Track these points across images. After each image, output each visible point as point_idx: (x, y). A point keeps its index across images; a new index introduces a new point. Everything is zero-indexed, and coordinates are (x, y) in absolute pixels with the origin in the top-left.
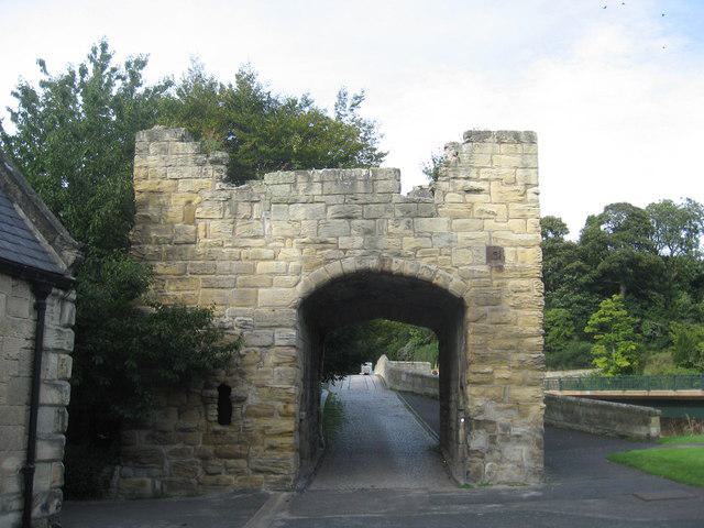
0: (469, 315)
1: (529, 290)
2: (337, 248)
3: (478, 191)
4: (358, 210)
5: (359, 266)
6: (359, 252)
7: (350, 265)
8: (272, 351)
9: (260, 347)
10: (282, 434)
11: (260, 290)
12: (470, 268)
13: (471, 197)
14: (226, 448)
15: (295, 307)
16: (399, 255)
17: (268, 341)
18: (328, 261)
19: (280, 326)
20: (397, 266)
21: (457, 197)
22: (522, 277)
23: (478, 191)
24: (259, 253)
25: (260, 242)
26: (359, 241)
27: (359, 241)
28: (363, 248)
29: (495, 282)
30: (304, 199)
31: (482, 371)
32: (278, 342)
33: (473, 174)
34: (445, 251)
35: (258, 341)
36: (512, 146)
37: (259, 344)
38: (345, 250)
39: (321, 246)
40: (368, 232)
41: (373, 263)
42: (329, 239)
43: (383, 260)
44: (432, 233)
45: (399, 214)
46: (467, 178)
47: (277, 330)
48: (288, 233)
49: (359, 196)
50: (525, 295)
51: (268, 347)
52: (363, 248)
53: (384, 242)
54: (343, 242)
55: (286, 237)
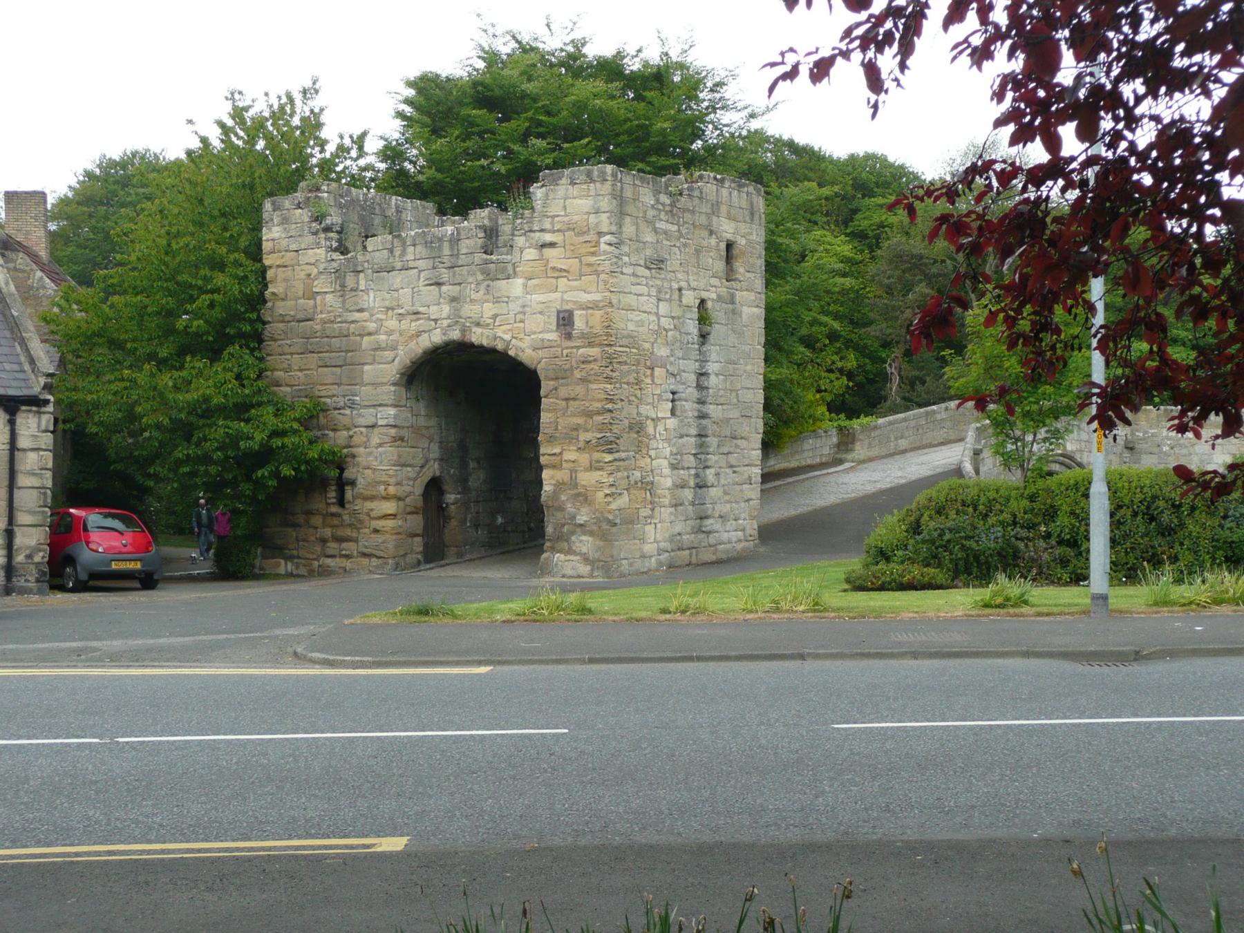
0: (542, 392)
1: (595, 360)
2: (429, 319)
3: (552, 245)
4: (445, 275)
5: (445, 338)
6: (446, 323)
7: (437, 338)
8: (376, 430)
9: (367, 427)
10: (385, 517)
11: (366, 368)
12: (540, 336)
13: (548, 252)
14: (340, 533)
15: (394, 384)
16: (478, 324)
17: (371, 421)
18: (419, 334)
19: (380, 405)
20: (478, 337)
21: (530, 254)
22: (591, 345)
23: (552, 245)
24: (364, 327)
25: (366, 315)
26: (446, 309)
27: (446, 309)
28: (449, 318)
29: (565, 352)
30: (399, 265)
31: (549, 452)
32: (380, 422)
33: (547, 226)
34: (519, 317)
35: (362, 421)
36: (584, 186)
37: (363, 424)
38: (436, 321)
39: (414, 317)
40: (454, 299)
41: (455, 335)
42: (421, 309)
43: (463, 331)
44: (508, 297)
45: (480, 277)
46: (542, 230)
47: (380, 409)
48: (387, 303)
49: (446, 259)
50: (592, 366)
51: (373, 426)
52: (449, 318)
53: (468, 310)
54: (434, 311)
55: (388, 309)
